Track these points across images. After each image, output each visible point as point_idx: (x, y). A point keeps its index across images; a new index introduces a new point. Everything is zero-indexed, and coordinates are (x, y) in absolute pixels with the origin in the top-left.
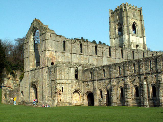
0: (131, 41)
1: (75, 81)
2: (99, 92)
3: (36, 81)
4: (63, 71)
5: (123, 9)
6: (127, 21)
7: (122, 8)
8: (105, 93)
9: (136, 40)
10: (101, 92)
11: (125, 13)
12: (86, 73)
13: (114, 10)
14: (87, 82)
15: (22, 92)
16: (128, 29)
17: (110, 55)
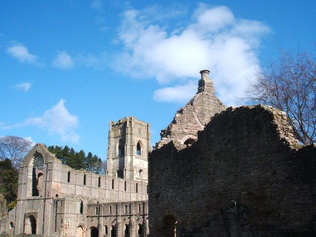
0: (134, 165)
1: (79, 216)
2: (104, 228)
3: (35, 213)
4: (70, 205)
5: (128, 124)
6: (131, 139)
7: (126, 122)
8: (110, 229)
9: (139, 163)
10: (106, 228)
11: (129, 129)
12: (91, 208)
13: (115, 123)
14: (92, 217)
15: (12, 224)
16: (132, 150)
17: (113, 188)
